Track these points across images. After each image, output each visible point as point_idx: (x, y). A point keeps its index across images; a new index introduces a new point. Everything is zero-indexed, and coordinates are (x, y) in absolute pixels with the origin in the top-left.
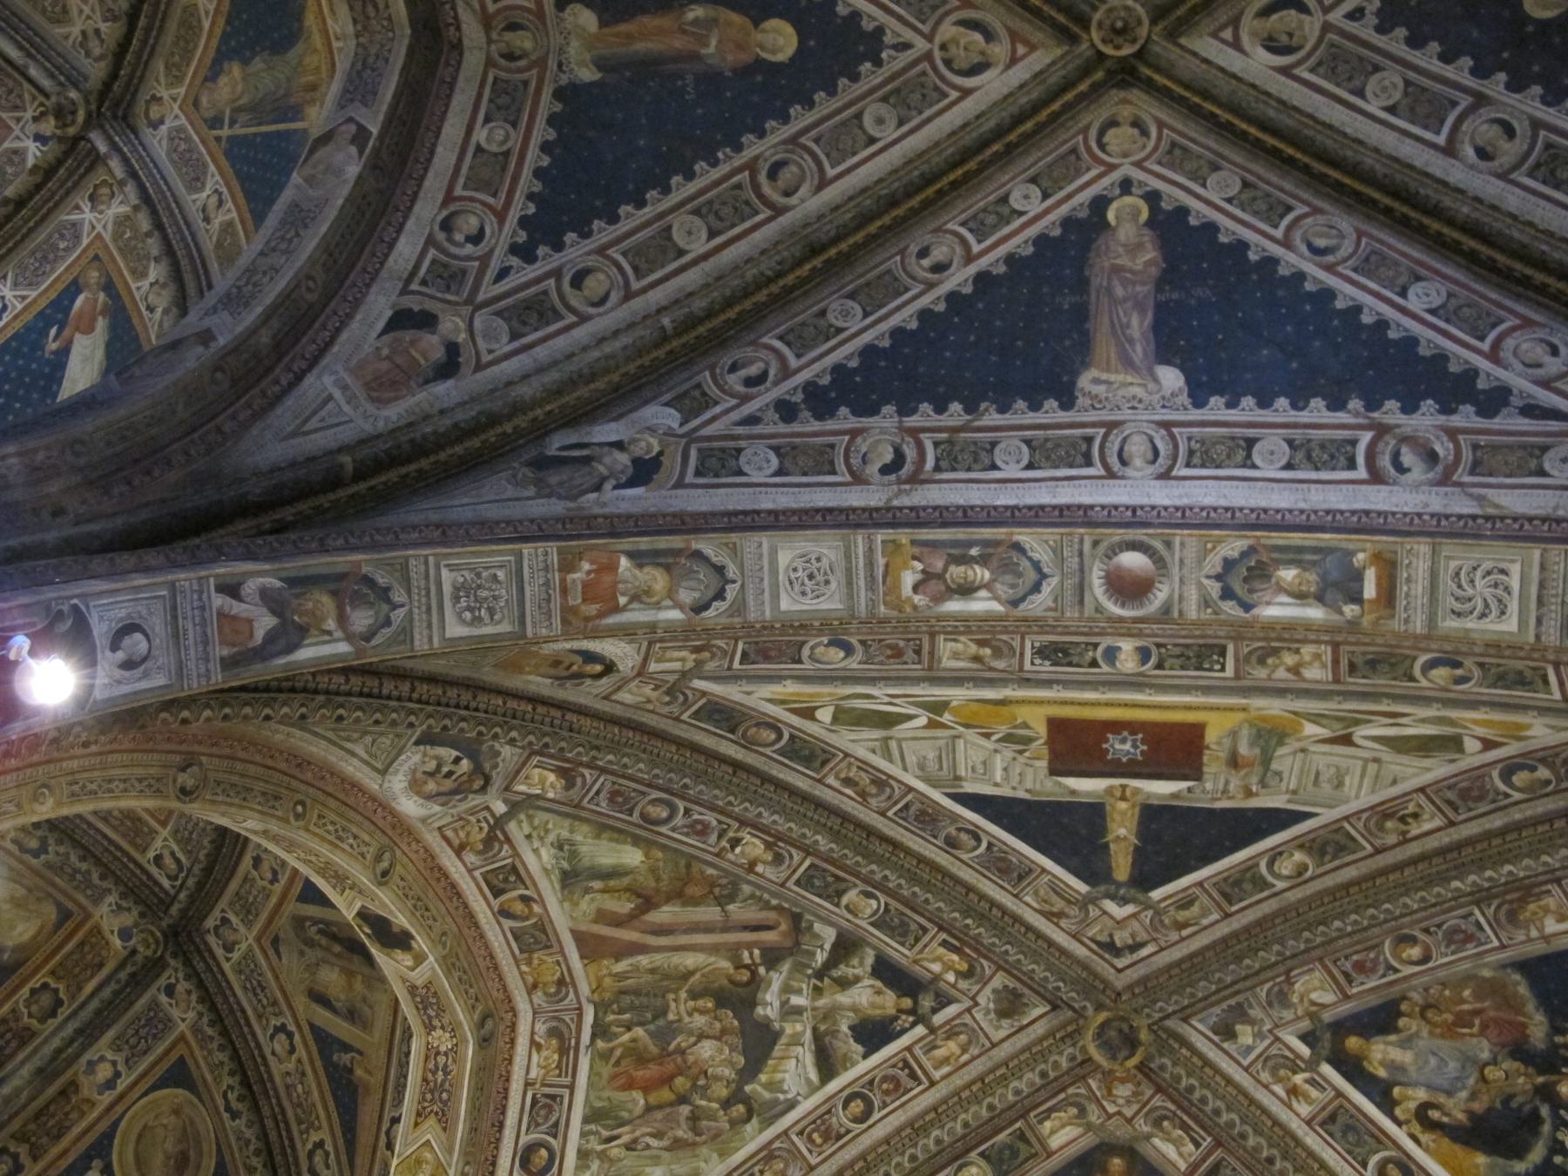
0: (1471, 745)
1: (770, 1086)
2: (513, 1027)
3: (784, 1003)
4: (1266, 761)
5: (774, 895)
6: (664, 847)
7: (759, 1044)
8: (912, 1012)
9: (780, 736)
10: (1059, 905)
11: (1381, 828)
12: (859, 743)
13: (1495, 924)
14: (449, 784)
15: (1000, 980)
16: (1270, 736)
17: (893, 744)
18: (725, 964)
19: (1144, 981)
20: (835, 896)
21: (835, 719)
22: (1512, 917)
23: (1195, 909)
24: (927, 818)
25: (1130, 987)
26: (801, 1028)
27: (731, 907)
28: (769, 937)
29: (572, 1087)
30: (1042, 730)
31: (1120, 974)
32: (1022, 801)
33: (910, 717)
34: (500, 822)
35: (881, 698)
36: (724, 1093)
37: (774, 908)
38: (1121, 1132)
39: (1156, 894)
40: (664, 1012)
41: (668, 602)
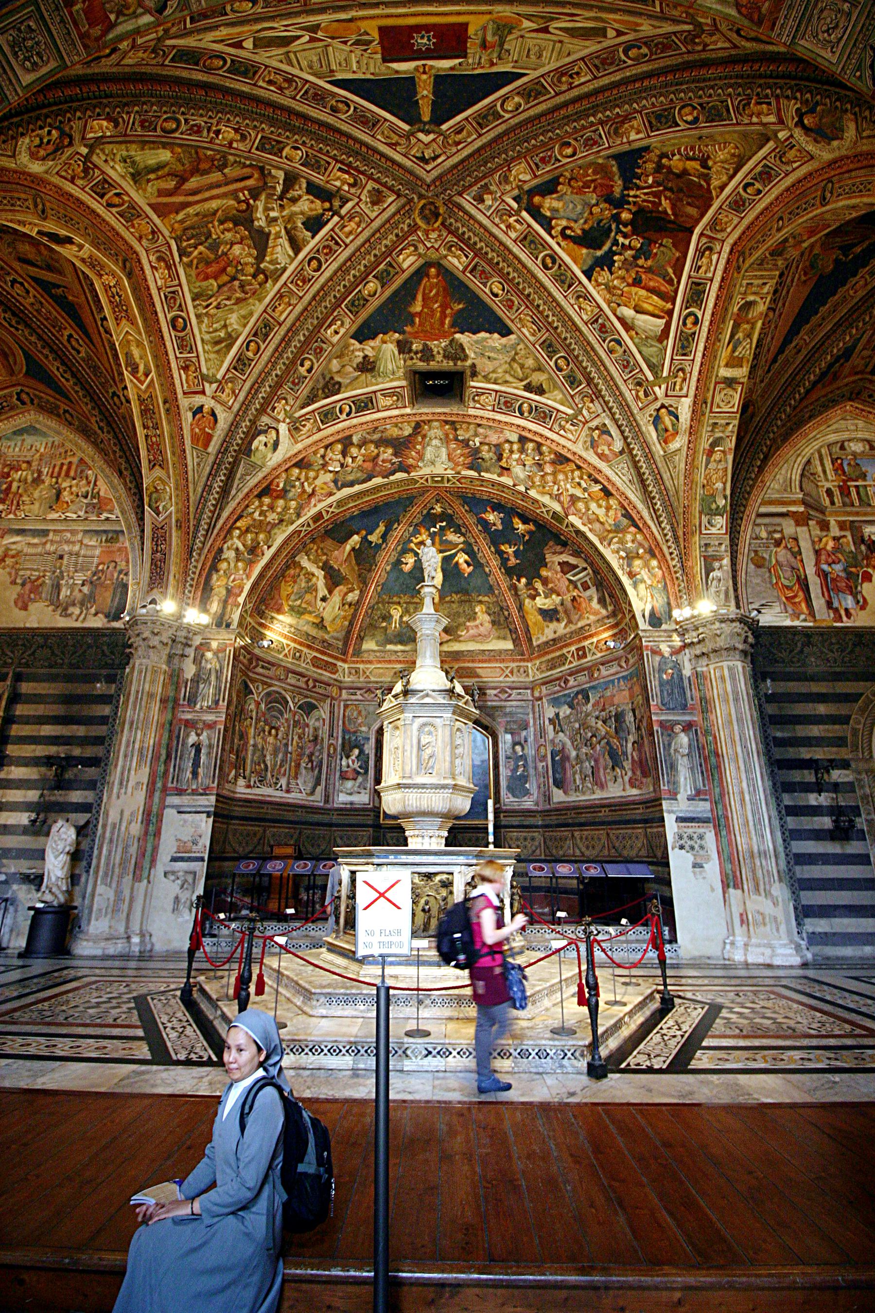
0: (611, 33)
1: (271, 262)
2: (139, 261)
3: (267, 217)
4: (501, 45)
5: (246, 158)
6: (180, 146)
7: (261, 241)
8: (330, 209)
9: (225, 62)
10: (396, 138)
11: (560, 81)
12: (271, 58)
13: (608, 134)
14: (51, 148)
15: (371, 185)
16: (504, 28)
17: (292, 56)
18: (232, 202)
19: (440, 177)
20: (279, 153)
21: (255, 46)
22: (616, 132)
23: (464, 133)
24: (319, 97)
25: (434, 181)
26: (277, 229)
27: (226, 171)
28: (250, 182)
29: (180, 285)
30: (376, 35)
31: (429, 174)
32: (368, 80)
33: (299, 37)
34: (87, 158)
35: (279, 28)
36: (252, 271)
37: (251, 166)
38: (433, 255)
39: (444, 127)
40: (209, 235)
41: (140, 10)
